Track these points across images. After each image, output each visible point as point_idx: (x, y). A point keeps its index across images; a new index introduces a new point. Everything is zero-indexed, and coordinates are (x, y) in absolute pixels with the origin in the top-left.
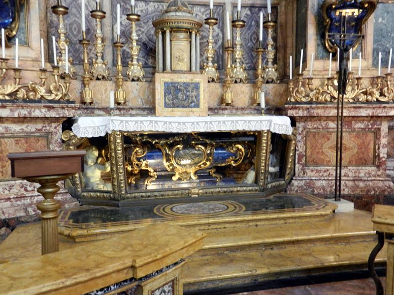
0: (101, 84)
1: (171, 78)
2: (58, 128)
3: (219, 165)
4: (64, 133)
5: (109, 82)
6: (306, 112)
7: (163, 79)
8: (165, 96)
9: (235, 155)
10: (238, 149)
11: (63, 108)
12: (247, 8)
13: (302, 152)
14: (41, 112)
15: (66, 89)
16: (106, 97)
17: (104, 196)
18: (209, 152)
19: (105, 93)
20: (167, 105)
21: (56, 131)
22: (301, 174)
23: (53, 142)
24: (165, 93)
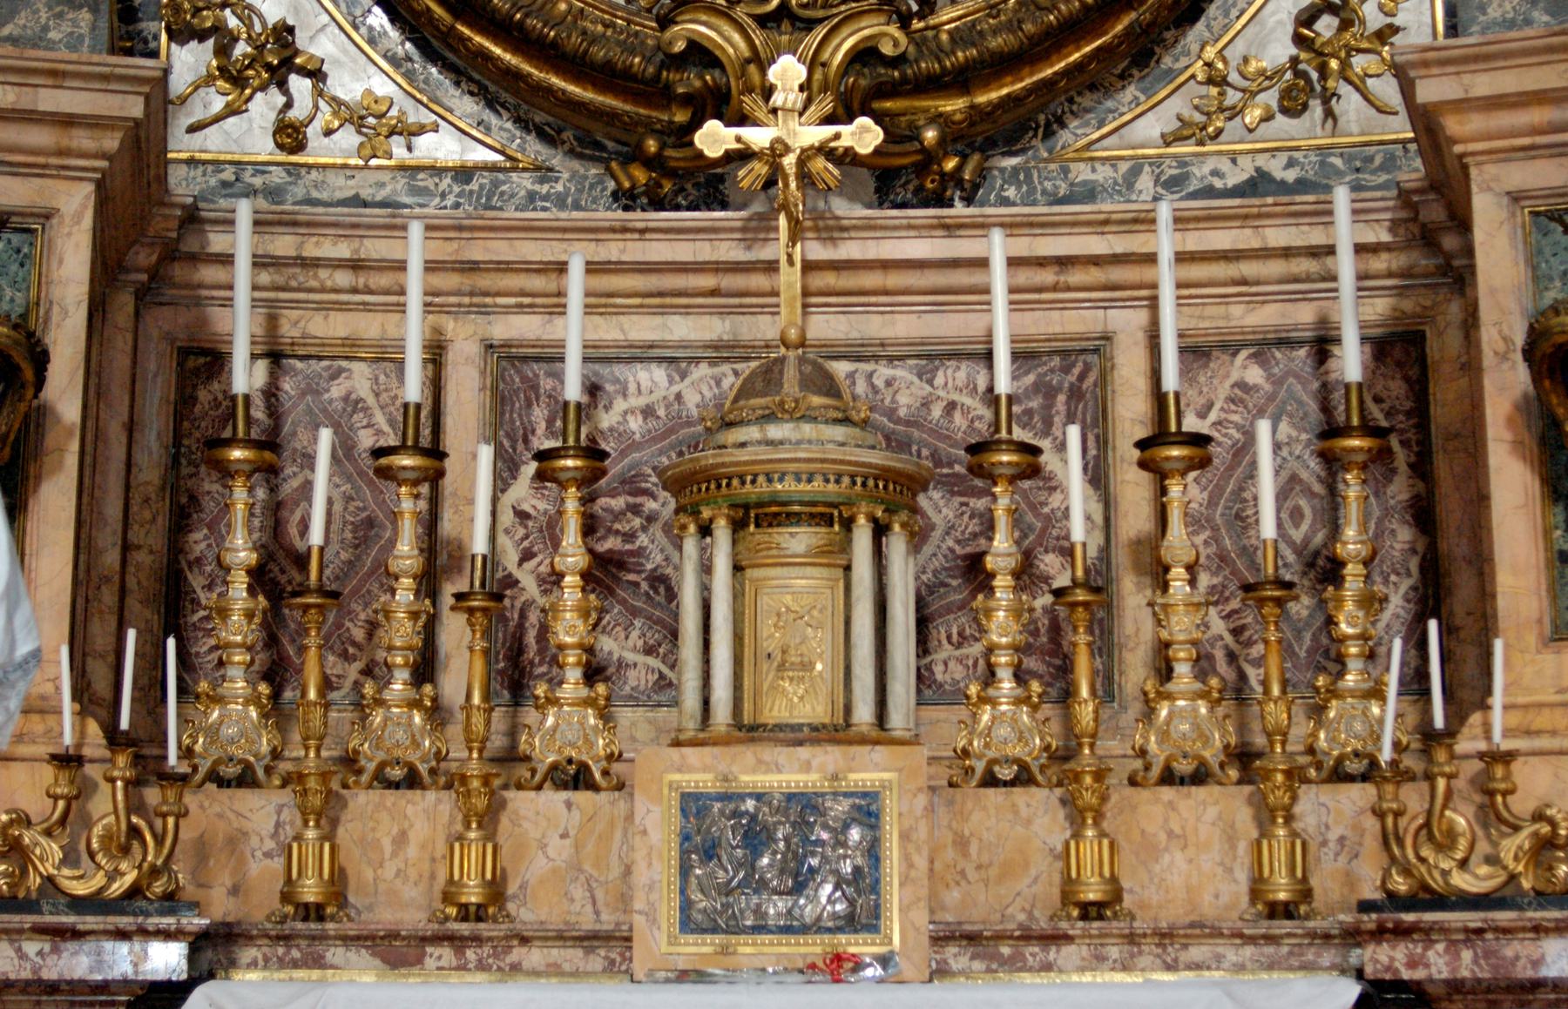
1: (722, 767)
5: (431, 795)
6: (1467, 955)
7: (677, 777)
8: (685, 871)
12: (1244, 354)
14: (22, 956)
15: (159, 840)
16: (398, 874)
19: (394, 854)
24: (684, 855)
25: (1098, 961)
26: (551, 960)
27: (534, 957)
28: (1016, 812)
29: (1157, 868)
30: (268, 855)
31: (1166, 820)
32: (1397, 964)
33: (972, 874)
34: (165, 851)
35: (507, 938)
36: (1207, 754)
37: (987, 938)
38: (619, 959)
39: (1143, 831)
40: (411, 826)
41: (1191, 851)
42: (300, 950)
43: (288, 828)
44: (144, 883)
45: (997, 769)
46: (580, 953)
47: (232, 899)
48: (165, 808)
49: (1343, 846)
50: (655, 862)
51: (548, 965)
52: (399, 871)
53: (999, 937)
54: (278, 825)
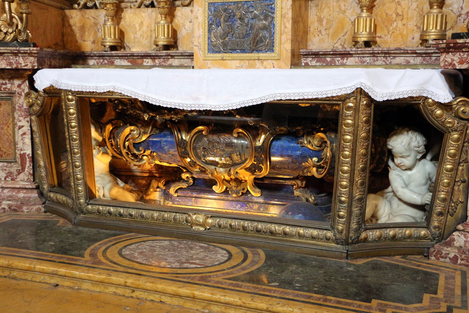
2: (22, 86)
8: (209, 31)
11: (16, 54)
19: (140, 30)
20: (213, 49)
21: (20, 91)
24: (210, 25)
25: (363, 65)
26: (181, 63)
28: (340, 9)
29: (391, 28)
32: (455, 62)
33: (324, 33)
40: (144, 20)
41: (405, 21)
42: (107, 60)
47: (93, 45)
50: (200, 28)
51: (180, 65)
52: (141, 35)
53: (326, 54)
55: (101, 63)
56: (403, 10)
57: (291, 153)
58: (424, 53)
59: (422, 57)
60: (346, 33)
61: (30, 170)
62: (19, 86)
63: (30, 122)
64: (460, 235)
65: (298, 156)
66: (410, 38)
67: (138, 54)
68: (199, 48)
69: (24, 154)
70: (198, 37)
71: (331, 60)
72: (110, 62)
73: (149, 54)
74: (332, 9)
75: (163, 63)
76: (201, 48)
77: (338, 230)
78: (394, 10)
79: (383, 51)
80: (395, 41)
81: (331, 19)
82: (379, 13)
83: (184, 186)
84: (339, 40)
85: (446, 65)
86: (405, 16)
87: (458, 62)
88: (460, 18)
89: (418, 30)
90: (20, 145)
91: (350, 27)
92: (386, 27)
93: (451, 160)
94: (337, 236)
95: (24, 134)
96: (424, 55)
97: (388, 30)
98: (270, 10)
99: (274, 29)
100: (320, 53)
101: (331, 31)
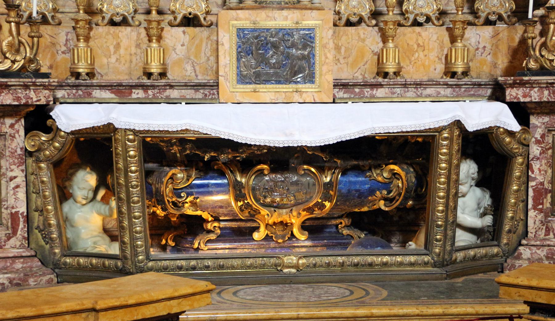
0: (108, 33)
1: (253, 18)
2: (16, 126)
3: (356, 210)
4: (27, 136)
6: (546, 92)
7: (235, 22)
8: (238, 60)
9: (387, 186)
10: (395, 175)
11: (26, 87)
13: (542, 184)
15: (32, 48)
17: (104, 264)
18: (328, 179)
19: (115, 53)
20: (242, 79)
21: (13, 132)
22: (542, 234)
23: (8, 154)
24: (239, 53)
26: (182, 95)
27: (174, 94)
28: (359, 37)
29: (413, 59)
30: (63, 53)
31: (417, 40)
32: (519, 96)
33: (342, 61)
34: (34, 52)
35: (165, 86)
36: (363, 14)
37: (350, 85)
38: (208, 94)
39: (408, 44)
40: (121, 41)
41: (426, 52)
42: (82, 91)
43: (71, 41)
44: (27, 65)
45: (418, 18)
46: (193, 91)
48: (33, 34)
49: (484, 50)
51: (181, 96)
53: (355, 85)
54: (67, 40)
55: (73, 94)
56: (424, 41)
57: (359, 187)
58: (455, 85)
59: (452, 88)
60: (367, 62)
61: (25, 233)
62: (12, 126)
63: (25, 172)
64: (525, 249)
65: (366, 190)
66: (432, 69)
67: (128, 84)
68: (226, 78)
69: (17, 213)
70: (224, 67)
71: (360, 91)
72: (87, 93)
73: (142, 84)
74: (350, 36)
75: (158, 95)
76: (227, 79)
77: (435, 253)
78: (415, 40)
79: (416, 83)
80: (417, 71)
81: (350, 47)
82: (401, 43)
83: (213, 236)
84: (359, 70)
85: (512, 99)
86: (426, 47)
87: (522, 96)
88: (478, 52)
89: (439, 61)
90: (11, 201)
91: (370, 56)
92: (408, 57)
93: (517, 181)
94: (435, 259)
95: (17, 187)
96: (454, 87)
97: (410, 60)
98: (309, 39)
99: (313, 60)
100: (350, 83)
101: (350, 60)
